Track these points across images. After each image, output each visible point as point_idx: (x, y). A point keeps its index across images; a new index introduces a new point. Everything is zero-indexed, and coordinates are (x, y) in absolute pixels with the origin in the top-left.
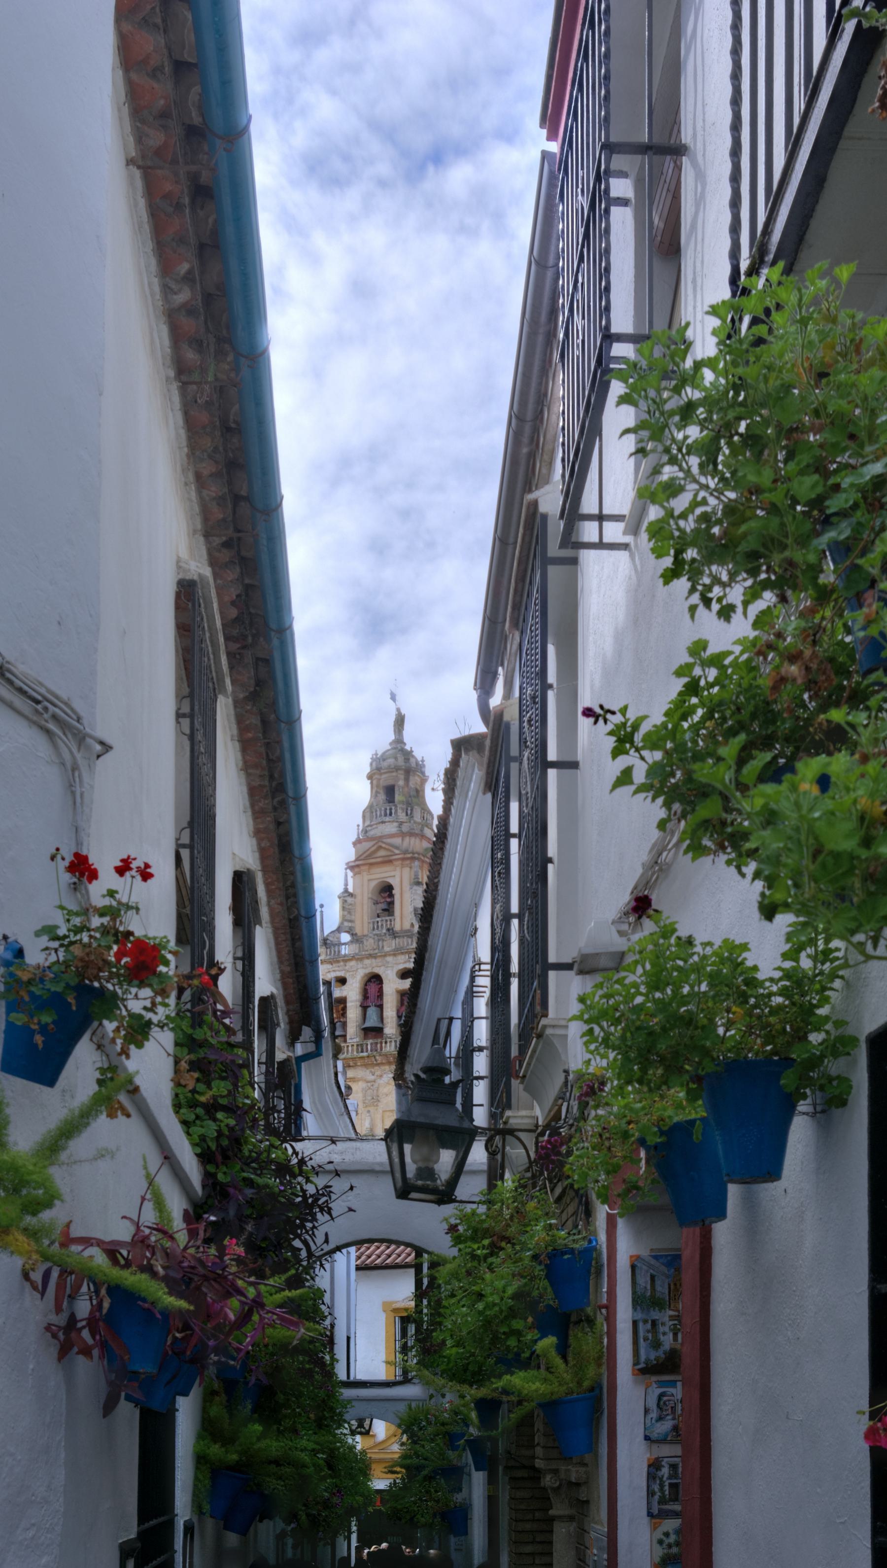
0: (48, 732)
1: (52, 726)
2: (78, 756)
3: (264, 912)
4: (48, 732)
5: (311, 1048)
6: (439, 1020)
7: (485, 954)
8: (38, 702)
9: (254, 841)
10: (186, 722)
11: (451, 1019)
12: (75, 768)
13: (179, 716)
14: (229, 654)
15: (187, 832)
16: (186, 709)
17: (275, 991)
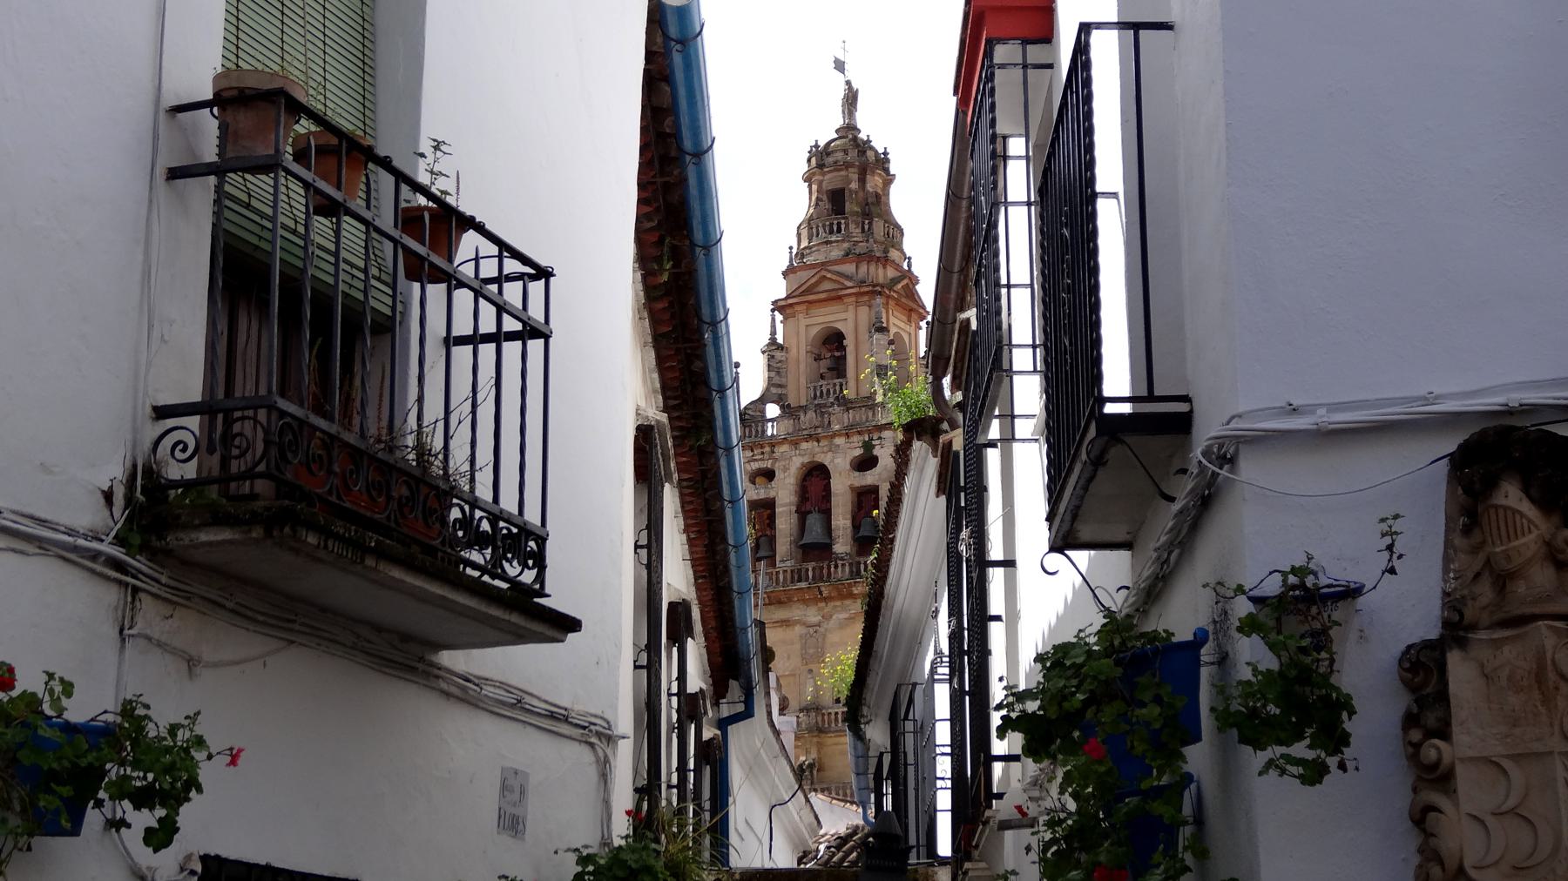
0: (592, 745)
1: (594, 740)
2: (609, 751)
3: (698, 627)
4: (592, 745)
5: (741, 708)
6: (899, 686)
7: (945, 646)
8: (584, 728)
9: (684, 537)
10: (644, 552)
11: (915, 685)
12: (606, 761)
13: (637, 547)
14: (674, 438)
15: (644, 656)
16: (644, 541)
17: (704, 687)
